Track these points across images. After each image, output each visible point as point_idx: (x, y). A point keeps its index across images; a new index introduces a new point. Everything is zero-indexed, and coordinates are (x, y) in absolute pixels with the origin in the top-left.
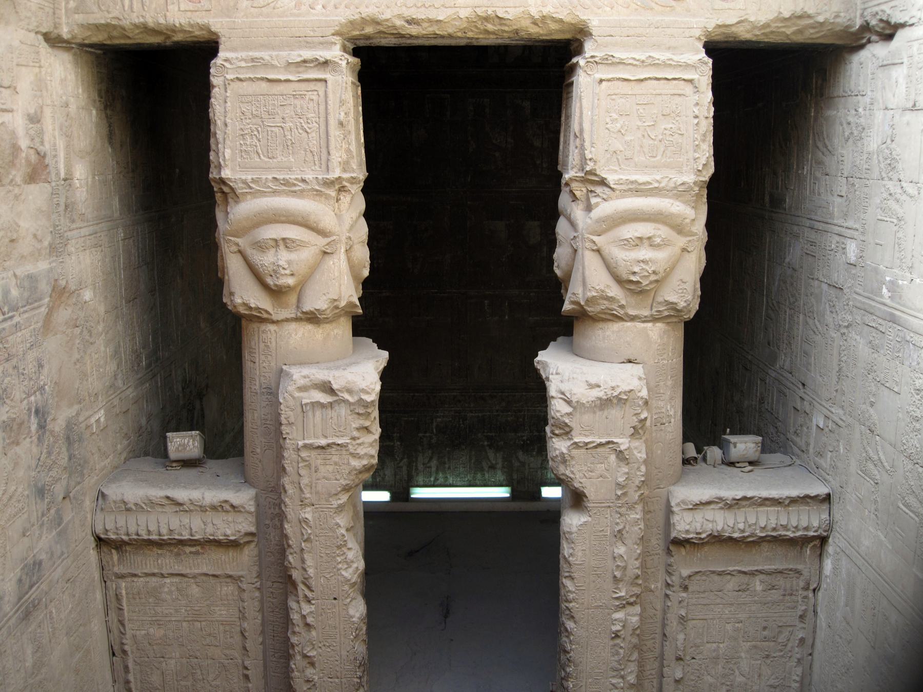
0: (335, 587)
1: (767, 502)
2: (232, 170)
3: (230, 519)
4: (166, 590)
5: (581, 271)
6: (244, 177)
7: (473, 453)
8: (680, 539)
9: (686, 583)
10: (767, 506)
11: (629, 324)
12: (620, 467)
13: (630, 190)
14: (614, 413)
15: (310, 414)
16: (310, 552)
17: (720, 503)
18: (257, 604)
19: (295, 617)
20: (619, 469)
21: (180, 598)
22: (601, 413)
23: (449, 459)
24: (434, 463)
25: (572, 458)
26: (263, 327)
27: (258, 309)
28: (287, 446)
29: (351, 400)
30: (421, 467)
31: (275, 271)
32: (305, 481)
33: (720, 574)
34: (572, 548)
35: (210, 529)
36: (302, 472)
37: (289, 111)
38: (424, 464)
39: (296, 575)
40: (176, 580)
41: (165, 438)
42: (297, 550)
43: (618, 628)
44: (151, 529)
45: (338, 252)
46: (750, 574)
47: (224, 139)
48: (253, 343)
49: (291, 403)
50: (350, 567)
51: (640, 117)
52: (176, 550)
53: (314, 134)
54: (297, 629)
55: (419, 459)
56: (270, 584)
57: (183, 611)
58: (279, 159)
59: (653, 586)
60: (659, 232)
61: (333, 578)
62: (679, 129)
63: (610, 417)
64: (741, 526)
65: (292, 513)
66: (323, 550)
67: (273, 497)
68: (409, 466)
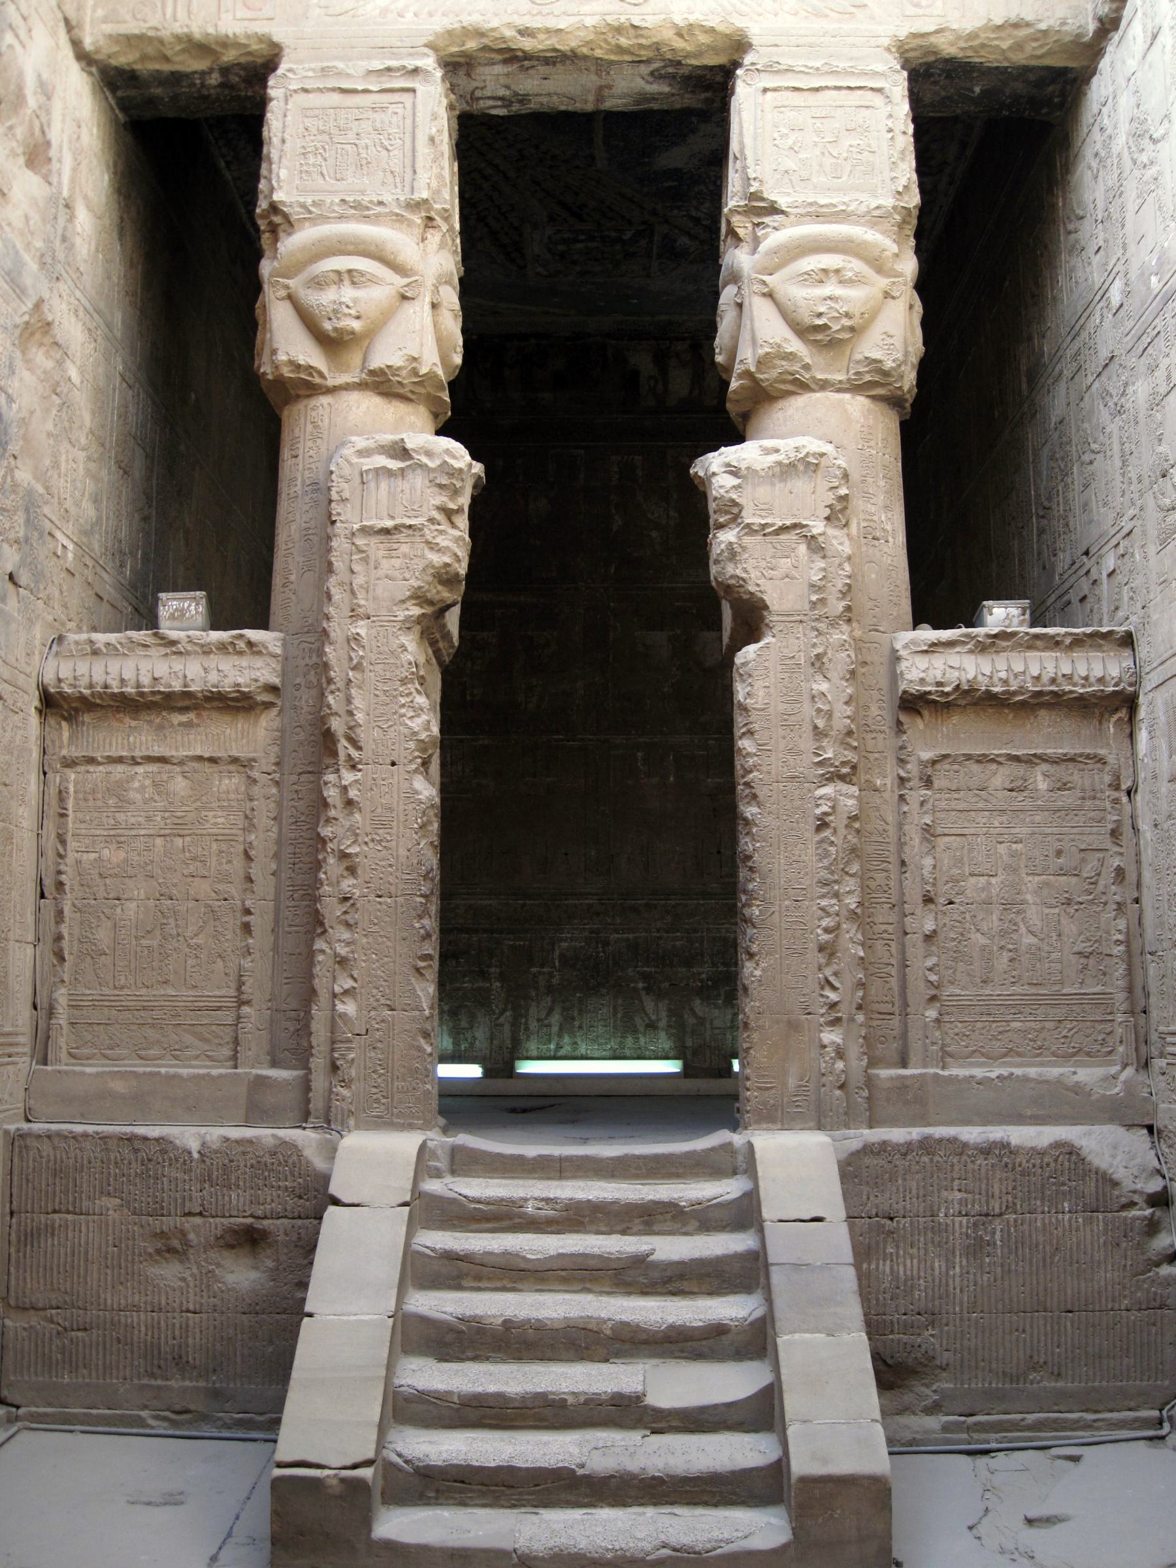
0: (393, 744)
1: (1039, 643)
2: (287, 193)
3: (244, 664)
4: (136, 785)
5: (749, 327)
6: (302, 200)
7: (620, 1001)
8: (912, 694)
9: (929, 771)
10: (1038, 649)
11: (818, 395)
12: (813, 561)
13: (808, 214)
14: (800, 485)
15: (372, 485)
16: (360, 688)
17: (967, 643)
18: (273, 805)
19: (332, 794)
20: (812, 565)
21: (156, 797)
22: (782, 485)
23: (580, 1010)
24: (555, 1019)
25: (744, 549)
26: (313, 402)
27: (309, 369)
28: (337, 531)
29: (431, 465)
30: (533, 1025)
31: (335, 311)
32: (359, 580)
33: (982, 759)
34: (751, 685)
35: (213, 678)
36: (356, 568)
37: (365, 125)
38: (538, 1020)
39: (337, 725)
40: (153, 768)
41: (157, 599)
42: (341, 684)
43: (825, 809)
44: (126, 677)
45: (421, 298)
46: (1026, 762)
47: (280, 157)
48: (297, 431)
49: (347, 471)
50: (418, 716)
51: (818, 132)
52: (158, 721)
53: (396, 152)
54: (332, 813)
55: (531, 1011)
56: (294, 778)
57: (159, 818)
58: (350, 181)
59: (878, 782)
60: (851, 265)
61: (392, 729)
62: (869, 146)
63: (795, 491)
64: (1003, 675)
65: (338, 630)
66: (380, 686)
67: (309, 640)
68: (515, 1024)
